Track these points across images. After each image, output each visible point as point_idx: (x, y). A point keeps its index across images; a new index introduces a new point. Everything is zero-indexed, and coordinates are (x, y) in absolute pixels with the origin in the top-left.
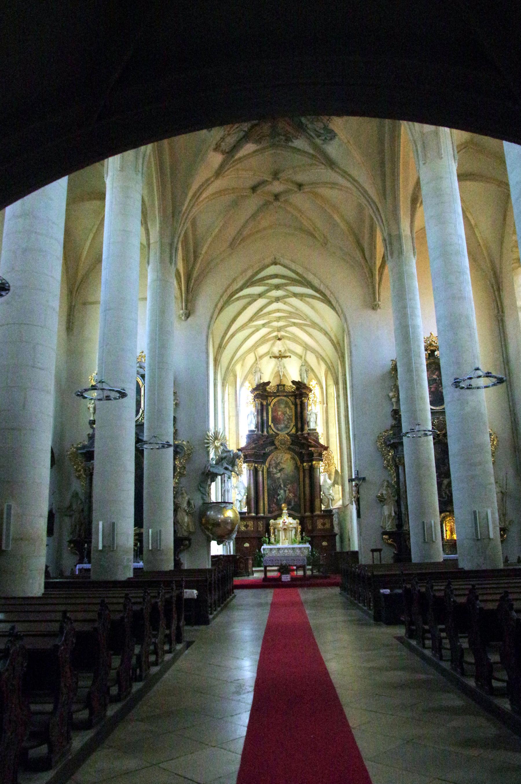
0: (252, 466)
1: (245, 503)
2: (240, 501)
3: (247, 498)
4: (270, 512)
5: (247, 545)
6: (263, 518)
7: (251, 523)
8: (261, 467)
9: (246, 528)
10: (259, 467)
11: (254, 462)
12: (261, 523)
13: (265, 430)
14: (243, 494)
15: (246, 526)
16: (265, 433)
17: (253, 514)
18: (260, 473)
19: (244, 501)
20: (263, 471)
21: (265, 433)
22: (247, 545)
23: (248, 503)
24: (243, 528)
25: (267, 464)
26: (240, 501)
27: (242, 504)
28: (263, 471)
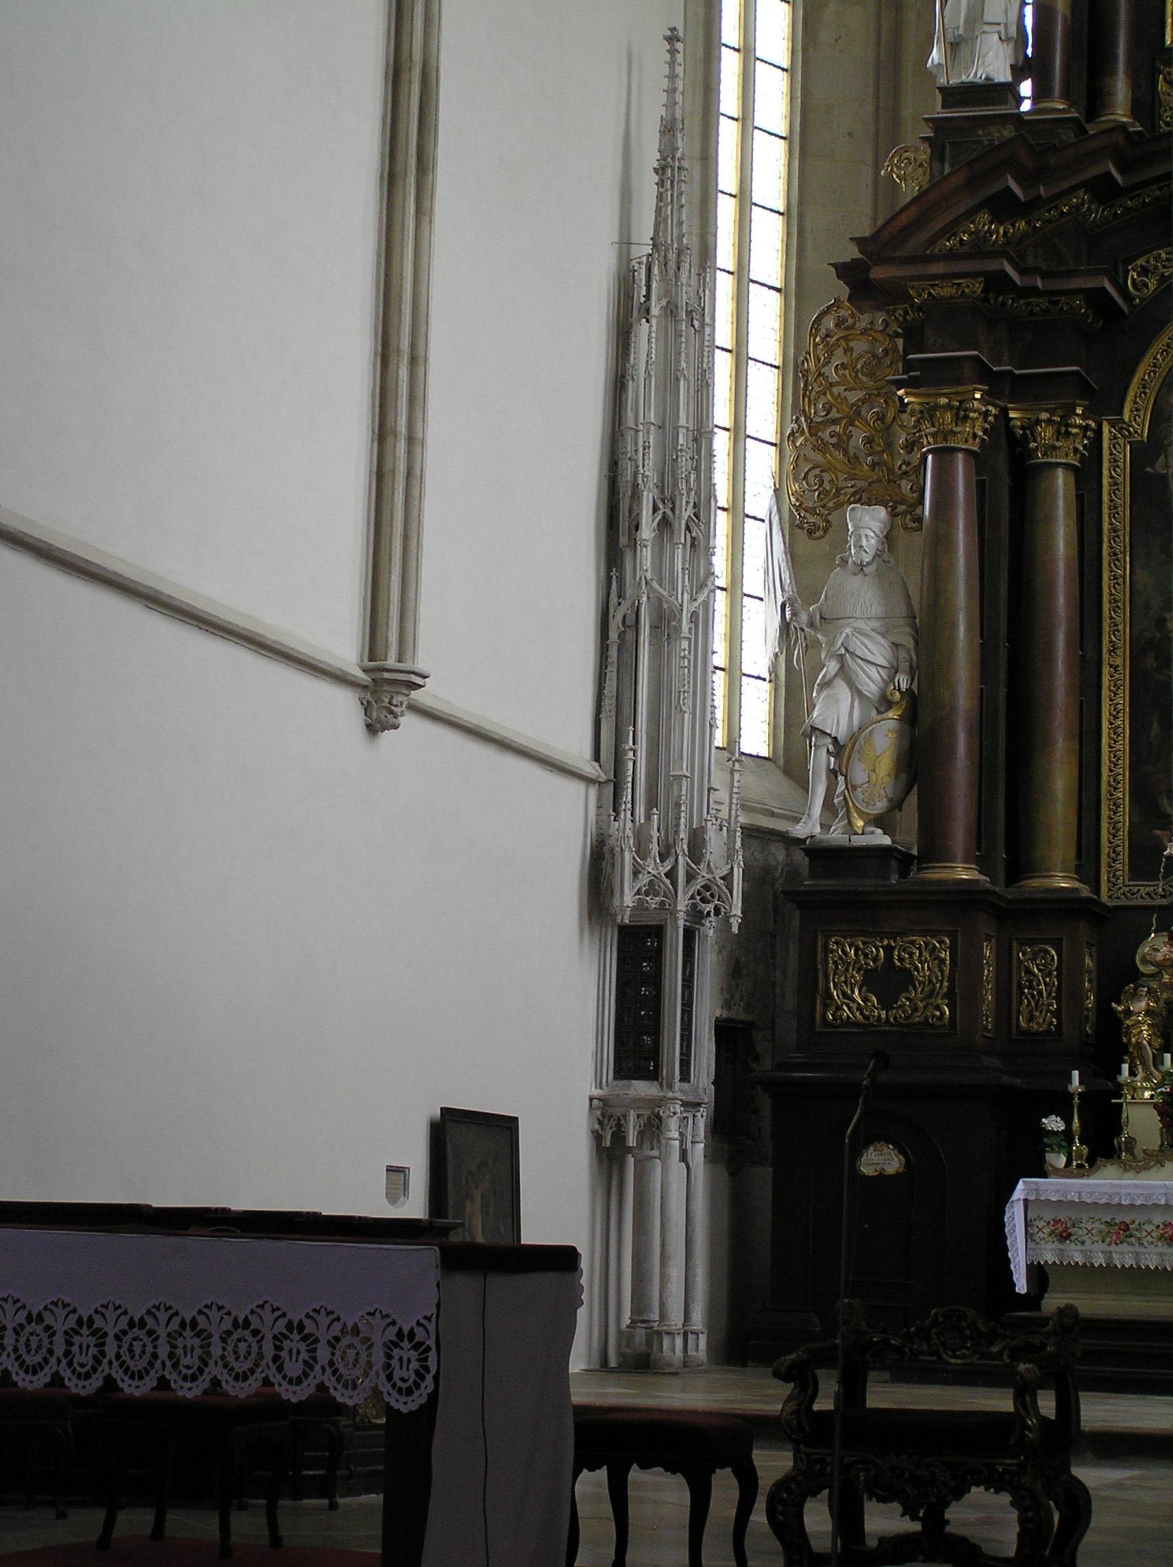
0: (961, 416)
1: (885, 765)
2: (838, 749)
3: (911, 718)
4: (1145, 859)
5: (880, 1160)
6: (1066, 908)
7: (926, 957)
8: (1062, 432)
9: (886, 1004)
10: (1046, 433)
11: (984, 375)
12: (1039, 968)
13: (1121, 88)
14: (871, 681)
15: (888, 981)
16: (1120, 109)
17: (964, 873)
18: (1062, 482)
19: (884, 739)
20: (1087, 475)
21: (1120, 109)
22: (880, 1160)
23: (919, 762)
24: (852, 1001)
25: (1136, 412)
26: (838, 749)
27: (860, 773)
28: (1087, 475)
